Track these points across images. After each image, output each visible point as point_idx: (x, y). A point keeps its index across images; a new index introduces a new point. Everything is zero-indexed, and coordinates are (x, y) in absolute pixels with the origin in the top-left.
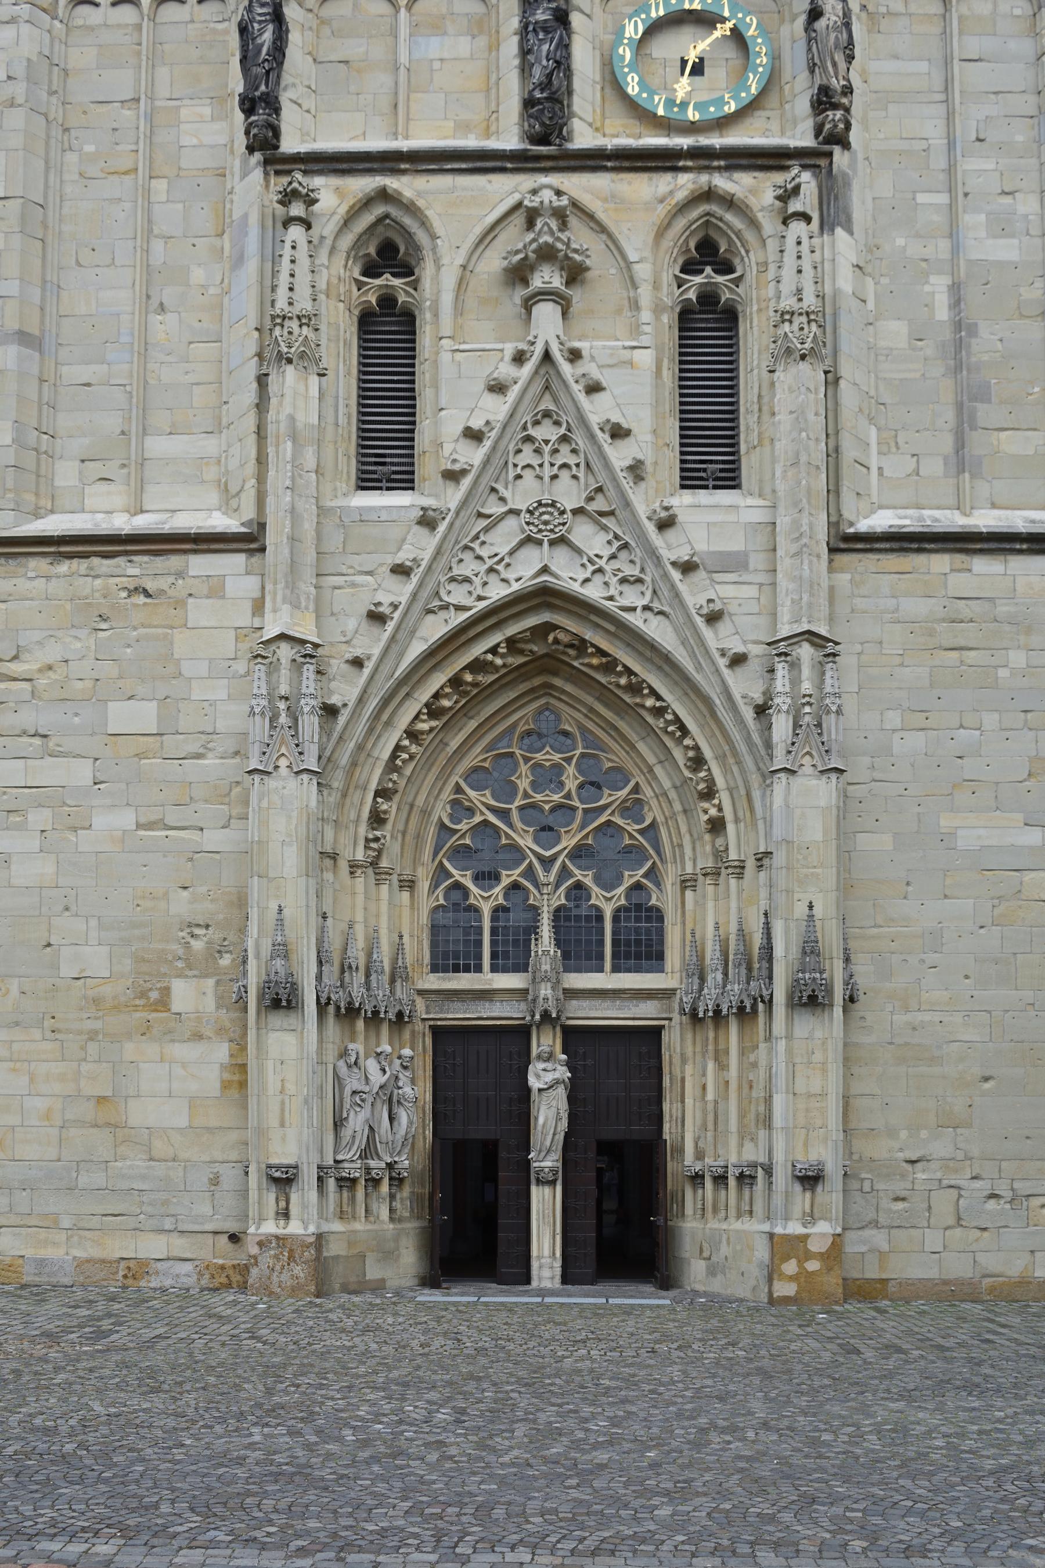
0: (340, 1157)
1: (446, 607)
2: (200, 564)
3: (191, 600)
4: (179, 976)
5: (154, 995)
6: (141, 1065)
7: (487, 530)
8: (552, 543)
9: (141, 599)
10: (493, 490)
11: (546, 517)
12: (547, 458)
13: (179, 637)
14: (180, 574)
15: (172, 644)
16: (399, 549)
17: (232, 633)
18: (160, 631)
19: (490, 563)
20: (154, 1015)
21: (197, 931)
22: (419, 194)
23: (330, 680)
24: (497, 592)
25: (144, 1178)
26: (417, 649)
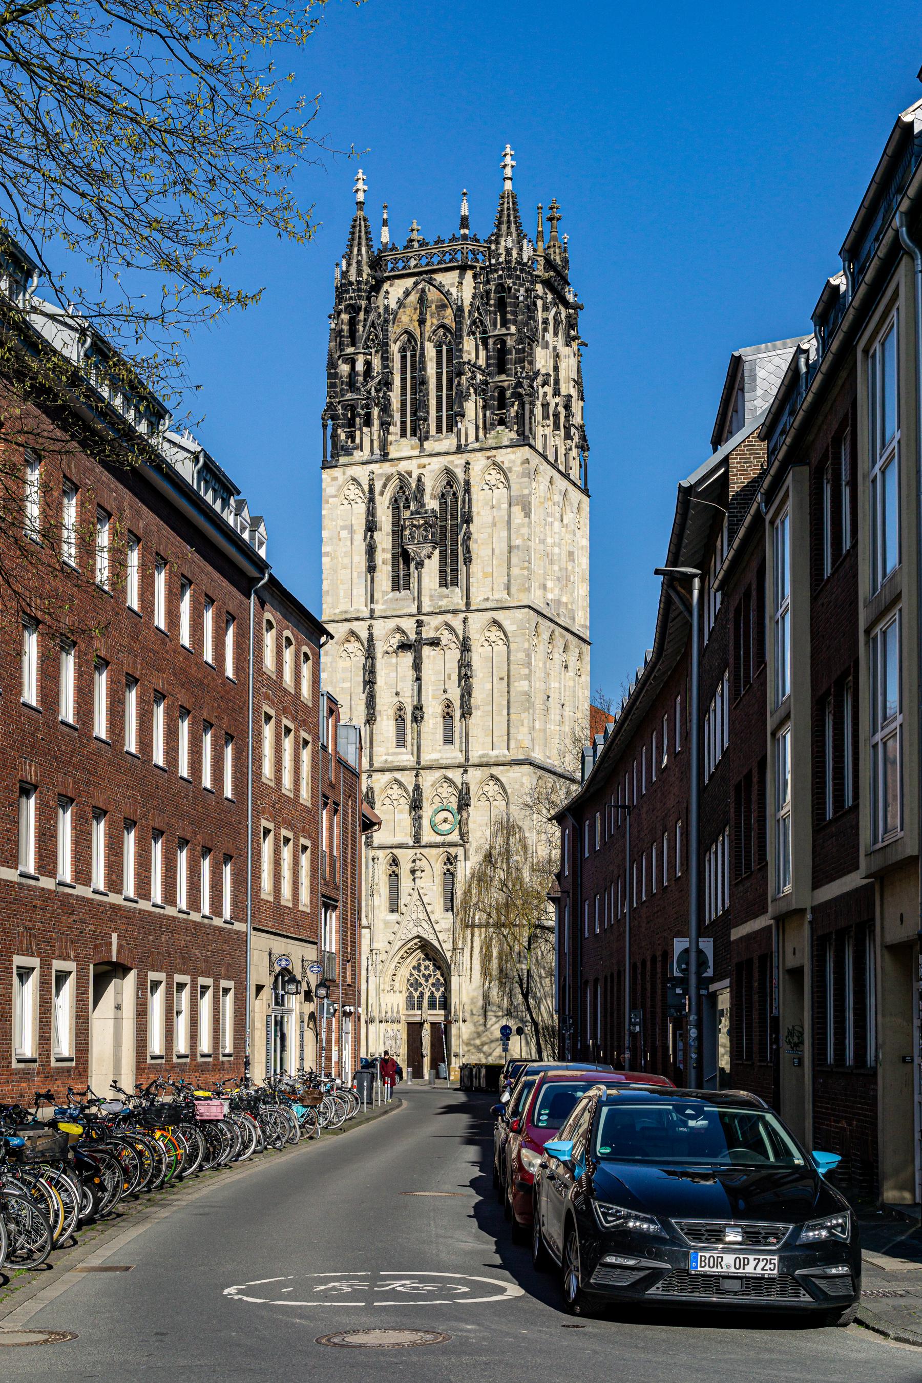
24: (410, 937)
26: (397, 948)
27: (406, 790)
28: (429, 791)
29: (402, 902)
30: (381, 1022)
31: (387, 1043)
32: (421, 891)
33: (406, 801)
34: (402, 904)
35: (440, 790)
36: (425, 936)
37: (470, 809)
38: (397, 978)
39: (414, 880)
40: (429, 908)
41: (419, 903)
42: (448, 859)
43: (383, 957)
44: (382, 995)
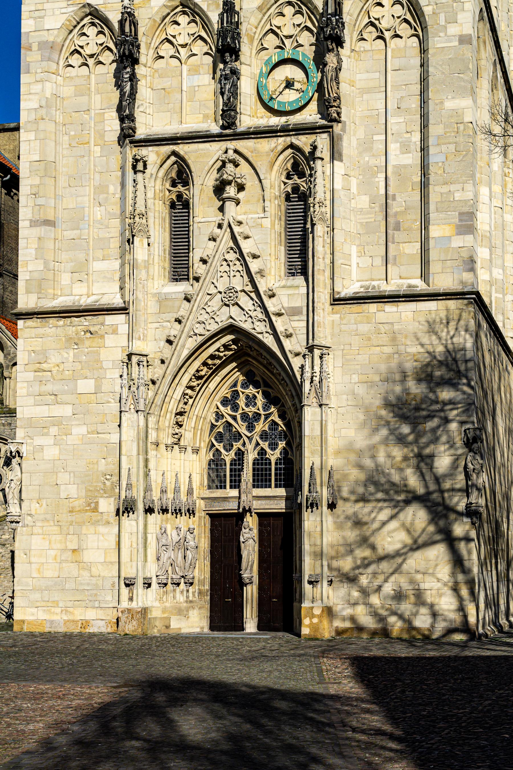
0: (158, 574)
1: (196, 335)
2: (110, 319)
3: (106, 336)
4: (101, 497)
5: (93, 505)
6: (89, 536)
7: (210, 300)
8: (233, 305)
9: (88, 335)
10: (213, 283)
11: (231, 295)
12: (232, 268)
13: (102, 351)
14: (103, 324)
15: (99, 354)
16: (179, 310)
17: (120, 349)
18: (95, 349)
19: (211, 314)
20: (93, 514)
21: (108, 477)
22: (186, 153)
23: (155, 368)
24: (214, 328)
25: (88, 584)
26: (186, 353)
27: (206, 24)
28: (254, 21)
29: (196, 255)
30: (149, 510)
31: (164, 557)
32: (236, 229)
33: (206, 49)
34: (197, 258)
35: (277, 21)
36: (247, 326)
37: (344, 52)
38: (189, 423)
39: (221, 209)
40: (254, 266)
41: (232, 256)
42: (296, 165)
43: (157, 371)
44: (152, 453)
